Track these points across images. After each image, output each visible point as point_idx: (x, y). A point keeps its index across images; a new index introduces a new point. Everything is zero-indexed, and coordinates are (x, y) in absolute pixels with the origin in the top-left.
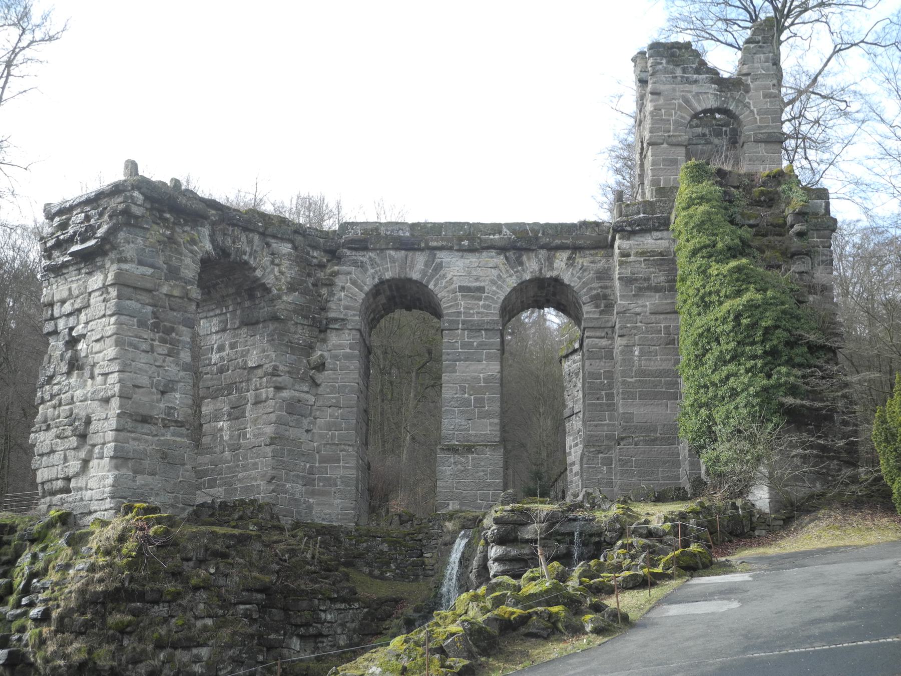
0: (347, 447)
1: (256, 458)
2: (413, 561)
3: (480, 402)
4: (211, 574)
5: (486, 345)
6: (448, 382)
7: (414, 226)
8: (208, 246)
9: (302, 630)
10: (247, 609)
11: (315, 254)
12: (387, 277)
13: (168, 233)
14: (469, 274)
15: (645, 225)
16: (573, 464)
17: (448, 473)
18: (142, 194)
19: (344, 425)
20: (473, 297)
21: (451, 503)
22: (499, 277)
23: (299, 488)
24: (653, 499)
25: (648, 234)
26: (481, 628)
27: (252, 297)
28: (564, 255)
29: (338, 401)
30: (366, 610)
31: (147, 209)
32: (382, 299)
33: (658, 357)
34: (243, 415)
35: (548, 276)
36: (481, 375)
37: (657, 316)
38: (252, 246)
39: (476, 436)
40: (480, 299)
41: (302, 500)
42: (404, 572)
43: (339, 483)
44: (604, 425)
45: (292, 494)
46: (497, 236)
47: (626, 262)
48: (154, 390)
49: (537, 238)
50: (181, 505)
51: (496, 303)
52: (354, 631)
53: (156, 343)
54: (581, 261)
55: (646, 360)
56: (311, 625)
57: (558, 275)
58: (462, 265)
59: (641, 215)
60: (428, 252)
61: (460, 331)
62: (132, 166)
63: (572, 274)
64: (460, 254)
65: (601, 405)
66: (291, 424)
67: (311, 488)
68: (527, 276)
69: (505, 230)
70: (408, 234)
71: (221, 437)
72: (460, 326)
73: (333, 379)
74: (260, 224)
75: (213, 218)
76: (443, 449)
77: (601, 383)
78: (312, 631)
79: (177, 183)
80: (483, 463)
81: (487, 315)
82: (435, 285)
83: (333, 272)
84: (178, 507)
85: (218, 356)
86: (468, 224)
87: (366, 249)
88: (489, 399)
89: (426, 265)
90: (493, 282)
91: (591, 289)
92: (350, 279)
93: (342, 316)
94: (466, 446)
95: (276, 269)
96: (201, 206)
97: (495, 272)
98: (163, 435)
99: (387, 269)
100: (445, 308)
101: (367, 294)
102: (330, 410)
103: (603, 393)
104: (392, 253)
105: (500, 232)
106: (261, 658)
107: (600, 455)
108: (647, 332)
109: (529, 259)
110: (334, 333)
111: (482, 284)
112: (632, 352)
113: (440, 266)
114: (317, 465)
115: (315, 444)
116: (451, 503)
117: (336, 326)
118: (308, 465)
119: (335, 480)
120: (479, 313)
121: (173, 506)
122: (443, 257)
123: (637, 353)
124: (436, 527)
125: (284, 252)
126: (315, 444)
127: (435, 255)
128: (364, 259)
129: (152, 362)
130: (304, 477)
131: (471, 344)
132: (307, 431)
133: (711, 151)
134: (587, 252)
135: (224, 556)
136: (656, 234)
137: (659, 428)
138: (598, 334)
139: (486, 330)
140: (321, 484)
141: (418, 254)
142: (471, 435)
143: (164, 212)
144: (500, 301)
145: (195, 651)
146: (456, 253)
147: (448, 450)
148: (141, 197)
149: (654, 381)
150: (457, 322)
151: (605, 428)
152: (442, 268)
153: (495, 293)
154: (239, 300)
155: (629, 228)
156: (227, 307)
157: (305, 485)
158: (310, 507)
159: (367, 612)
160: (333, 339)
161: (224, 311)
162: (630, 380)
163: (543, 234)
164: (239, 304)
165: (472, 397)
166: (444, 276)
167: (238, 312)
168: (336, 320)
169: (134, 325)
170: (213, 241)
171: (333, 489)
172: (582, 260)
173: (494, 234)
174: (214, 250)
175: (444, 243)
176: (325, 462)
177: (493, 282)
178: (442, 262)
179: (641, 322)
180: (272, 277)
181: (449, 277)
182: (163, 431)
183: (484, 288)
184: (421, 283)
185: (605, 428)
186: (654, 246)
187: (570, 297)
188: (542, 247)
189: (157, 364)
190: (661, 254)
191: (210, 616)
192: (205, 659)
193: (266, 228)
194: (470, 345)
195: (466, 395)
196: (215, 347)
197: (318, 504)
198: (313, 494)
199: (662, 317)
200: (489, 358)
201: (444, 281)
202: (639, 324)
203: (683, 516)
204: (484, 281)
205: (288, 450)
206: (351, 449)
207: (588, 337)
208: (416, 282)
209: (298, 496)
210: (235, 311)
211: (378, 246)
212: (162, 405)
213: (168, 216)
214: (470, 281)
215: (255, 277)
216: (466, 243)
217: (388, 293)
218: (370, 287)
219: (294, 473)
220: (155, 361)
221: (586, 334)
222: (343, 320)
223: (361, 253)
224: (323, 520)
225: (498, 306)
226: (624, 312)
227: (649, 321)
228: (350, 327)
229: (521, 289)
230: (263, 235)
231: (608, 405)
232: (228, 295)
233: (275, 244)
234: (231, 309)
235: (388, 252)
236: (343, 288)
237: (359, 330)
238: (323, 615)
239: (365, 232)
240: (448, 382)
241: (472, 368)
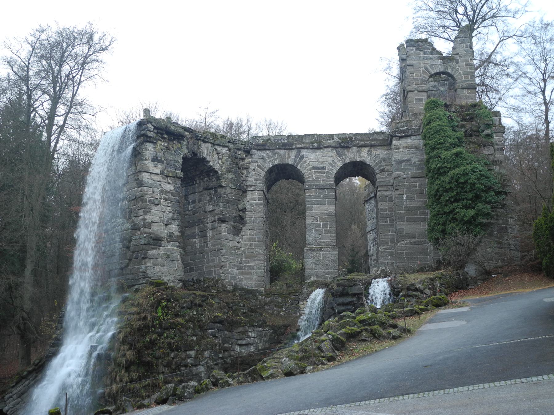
0: (259, 250)
1: (214, 256)
2: (294, 306)
3: (325, 225)
4: (194, 315)
5: (328, 196)
6: (309, 216)
7: (288, 137)
8: (186, 151)
9: (240, 342)
10: (213, 332)
11: (239, 153)
12: (276, 163)
13: (166, 144)
14: (318, 161)
15: (407, 132)
16: (372, 255)
18: (153, 126)
20: (320, 172)
22: (333, 161)
23: (235, 271)
24: (416, 271)
25: (409, 138)
26: (337, 337)
27: (208, 176)
28: (366, 150)
29: (253, 227)
30: (271, 331)
31: (155, 133)
32: (274, 175)
33: (416, 200)
34: (206, 236)
35: (358, 160)
36: (326, 212)
37: (415, 179)
38: (208, 150)
39: (324, 242)
40: (324, 173)
41: (237, 277)
42: (289, 311)
43: (255, 268)
44: (389, 235)
45: (232, 274)
46: (332, 141)
47: (398, 152)
48: (162, 224)
49: (352, 141)
50: (177, 281)
51: (332, 174)
52: (266, 342)
53: (162, 200)
54: (375, 152)
55: (410, 201)
56: (244, 339)
57: (363, 160)
59: (405, 128)
60: (296, 150)
61: (314, 190)
62: (146, 111)
63: (370, 159)
64: (313, 150)
65: (387, 225)
66: (230, 239)
67: (241, 271)
68: (348, 161)
69: (335, 137)
70: (286, 141)
71: (195, 246)
73: (250, 216)
74: (211, 139)
75: (188, 136)
76: (307, 250)
77: (387, 214)
78: (244, 342)
79: (169, 119)
80: (328, 256)
81: (327, 181)
82: (301, 167)
83: (248, 162)
84: (175, 282)
85: (192, 206)
86: (316, 135)
87: (265, 150)
88: (330, 224)
89: (296, 156)
90: (330, 164)
91: (380, 166)
93: (254, 184)
94: (319, 248)
95: (220, 161)
96: (181, 131)
97: (331, 159)
98: (167, 246)
100: (306, 178)
101: (266, 172)
102: (249, 232)
103: (388, 219)
104: (279, 151)
105: (333, 139)
106: (221, 356)
107: (387, 251)
108: (410, 187)
109: (348, 152)
110: (250, 192)
111: (325, 165)
112: (402, 198)
113: (303, 157)
114: (244, 259)
115: (243, 249)
117: (251, 189)
118: (239, 260)
119: (253, 267)
120: (323, 180)
121: (173, 281)
122: (304, 152)
123: (405, 198)
124: (305, 289)
125: (223, 152)
126: (243, 249)
127: (300, 151)
128: (264, 155)
129: (160, 210)
130: (238, 266)
131: (319, 196)
132: (238, 242)
133: (439, 93)
134: (378, 147)
135: (200, 306)
136: (413, 137)
137: (417, 236)
138: (385, 189)
139: (327, 189)
140: (246, 269)
141: (291, 151)
142: (321, 242)
143: (164, 134)
144: (334, 174)
145: (188, 353)
146: (311, 150)
147: (310, 250)
148: (152, 127)
149: (414, 212)
150: (312, 185)
151: (390, 237)
152: (304, 158)
153: (331, 170)
154: (202, 177)
155: (399, 135)
156: (196, 181)
157: (238, 270)
158: (241, 280)
159: (272, 332)
160: (249, 196)
161: (195, 183)
162: (401, 212)
163: (355, 139)
164: (202, 179)
166: (305, 162)
167: (202, 183)
168: (251, 186)
169: (150, 192)
170: (188, 148)
171: (253, 271)
172: (374, 152)
173: (330, 140)
174: (189, 152)
175: (305, 145)
177: (330, 164)
178: (304, 155)
179: (406, 182)
180: (218, 165)
181: (307, 162)
182: (167, 244)
183: (326, 167)
184: (293, 166)
185: (390, 237)
186: (412, 143)
187: (370, 171)
188: (355, 146)
189: (163, 211)
190: (416, 147)
191: (194, 335)
192: (193, 356)
193: (215, 141)
194: (319, 196)
196: (191, 201)
197: (245, 279)
198: (242, 274)
199: (417, 179)
200: (329, 203)
201: (305, 165)
202: (405, 183)
203: (432, 280)
204: (326, 164)
205: (229, 252)
206: (261, 251)
207: (379, 191)
208: (291, 165)
209: (235, 275)
210: (200, 183)
211: (271, 148)
212: (166, 231)
213: (166, 136)
214: (318, 164)
215: (210, 165)
216: (316, 145)
217: (277, 171)
218: (268, 169)
219: (233, 264)
220: (162, 209)
221: (379, 189)
222: (254, 186)
223: (262, 152)
224: (248, 286)
225: (333, 176)
226: (397, 178)
227: (411, 182)
229: (345, 167)
230: (213, 144)
231: (391, 225)
232: (196, 175)
233: (219, 148)
234: (198, 182)
235: (276, 151)
236: (254, 170)
237: (263, 191)
238: (250, 334)
239: (264, 141)
240: (309, 216)
241: (321, 208)
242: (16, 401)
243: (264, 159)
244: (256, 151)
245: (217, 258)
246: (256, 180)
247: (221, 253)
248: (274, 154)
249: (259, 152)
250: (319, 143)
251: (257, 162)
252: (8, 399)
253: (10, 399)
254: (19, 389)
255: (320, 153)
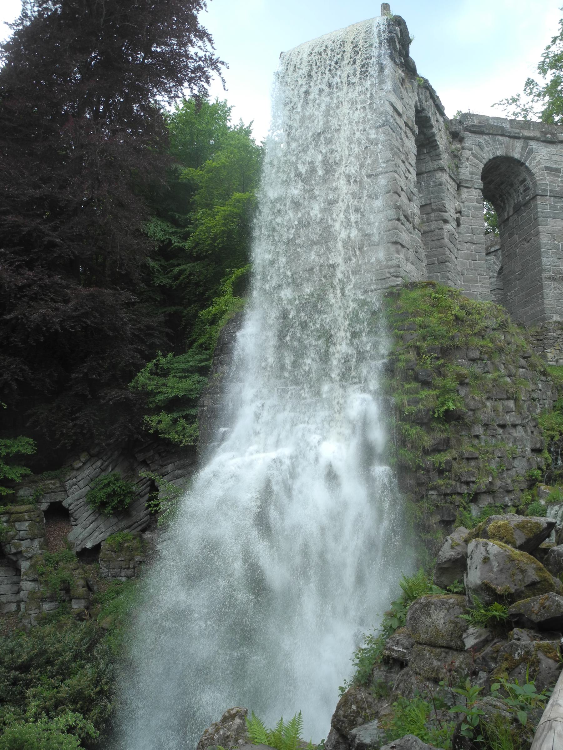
6: (544, 232)
14: (550, 159)
17: (551, 295)
19: (477, 257)
20: (554, 175)
21: (554, 315)
40: (558, 177)
58: (545, 152)
61: (548, 197)
64: (544, 144)
72: (549, 194)
73: (468, 222)
82: (530, 164)
92: (472, 153)
99: (497, 149)
100: (538, 180)
102: (467, 245)
110: (465, 190)
111: (559, 167)
113: (531, 151)
116: (554, 315)
122: (533, 144)
127: (528, 143)
128: (481, 140)
131: (555, 207)
146: (541, 143)
147: (549, 278)
150: (546, 190)
165: (560, 244)
166: (534, 158)
176: (467, 282)
178: (532, 149)
181: (538, 159)
194: (554, 207)
195: (556, 242)
211: (491, 132)
216: (549, 136)
218: (487, 160)
223: (478, 136)
228: (476, 187)
241: (558, 223)
242: (83, 490)
243: (479, 145)
244: (470, 135)
245: (439, 274)
246: (471, 173)
247: (447, 267)
248: (494, 141)
249: (473, 135)
250: (553, 134)
251: (471, 149)
252: (71, 487)
253: (74, 487)
254: (87, 472)
255: (552, 149)
